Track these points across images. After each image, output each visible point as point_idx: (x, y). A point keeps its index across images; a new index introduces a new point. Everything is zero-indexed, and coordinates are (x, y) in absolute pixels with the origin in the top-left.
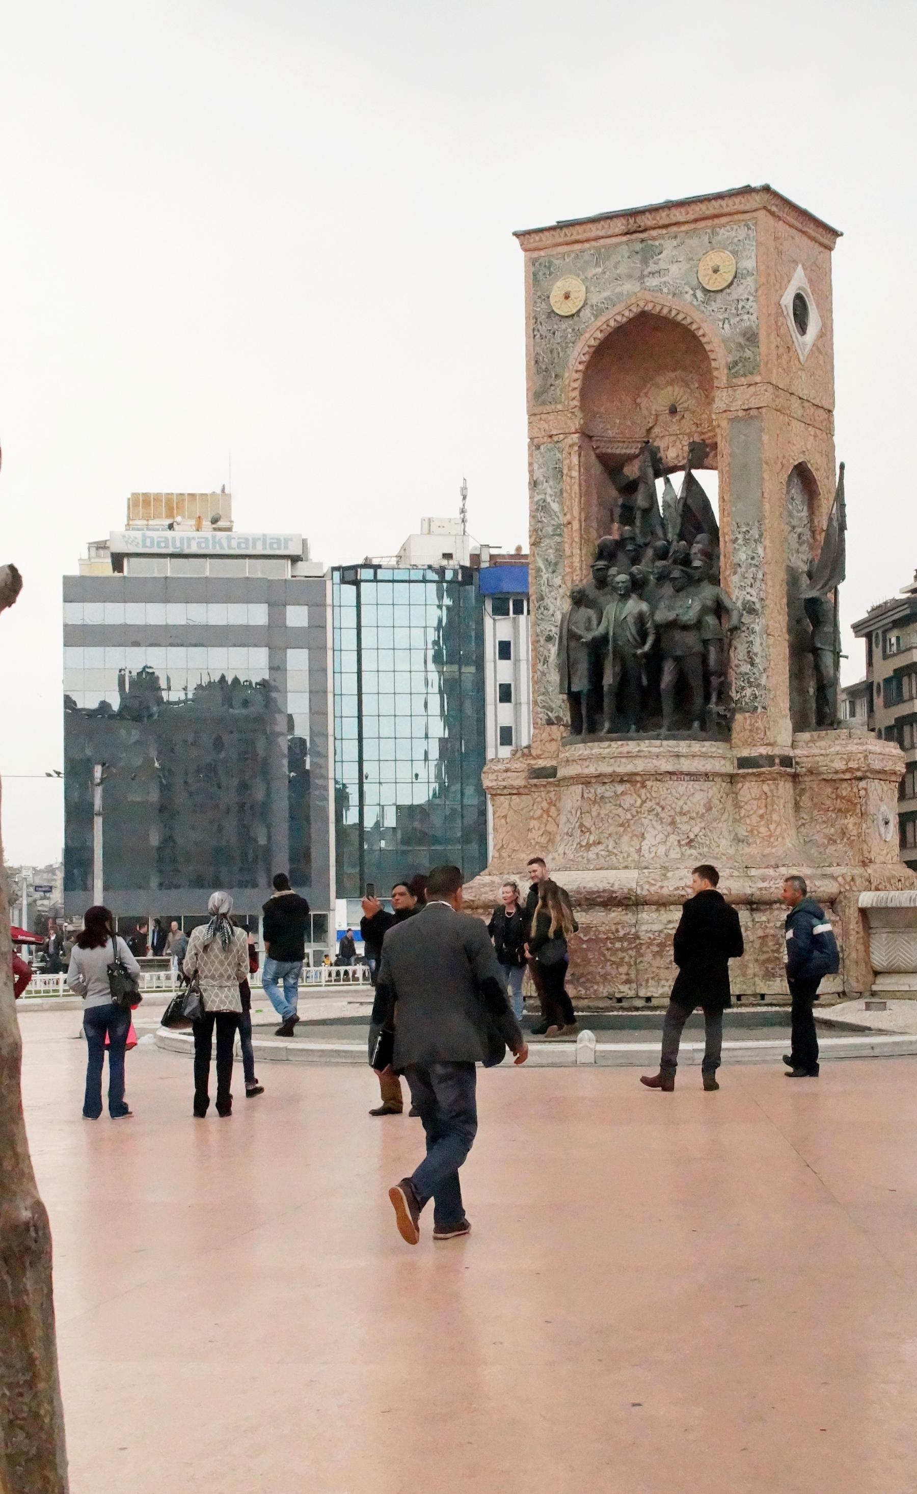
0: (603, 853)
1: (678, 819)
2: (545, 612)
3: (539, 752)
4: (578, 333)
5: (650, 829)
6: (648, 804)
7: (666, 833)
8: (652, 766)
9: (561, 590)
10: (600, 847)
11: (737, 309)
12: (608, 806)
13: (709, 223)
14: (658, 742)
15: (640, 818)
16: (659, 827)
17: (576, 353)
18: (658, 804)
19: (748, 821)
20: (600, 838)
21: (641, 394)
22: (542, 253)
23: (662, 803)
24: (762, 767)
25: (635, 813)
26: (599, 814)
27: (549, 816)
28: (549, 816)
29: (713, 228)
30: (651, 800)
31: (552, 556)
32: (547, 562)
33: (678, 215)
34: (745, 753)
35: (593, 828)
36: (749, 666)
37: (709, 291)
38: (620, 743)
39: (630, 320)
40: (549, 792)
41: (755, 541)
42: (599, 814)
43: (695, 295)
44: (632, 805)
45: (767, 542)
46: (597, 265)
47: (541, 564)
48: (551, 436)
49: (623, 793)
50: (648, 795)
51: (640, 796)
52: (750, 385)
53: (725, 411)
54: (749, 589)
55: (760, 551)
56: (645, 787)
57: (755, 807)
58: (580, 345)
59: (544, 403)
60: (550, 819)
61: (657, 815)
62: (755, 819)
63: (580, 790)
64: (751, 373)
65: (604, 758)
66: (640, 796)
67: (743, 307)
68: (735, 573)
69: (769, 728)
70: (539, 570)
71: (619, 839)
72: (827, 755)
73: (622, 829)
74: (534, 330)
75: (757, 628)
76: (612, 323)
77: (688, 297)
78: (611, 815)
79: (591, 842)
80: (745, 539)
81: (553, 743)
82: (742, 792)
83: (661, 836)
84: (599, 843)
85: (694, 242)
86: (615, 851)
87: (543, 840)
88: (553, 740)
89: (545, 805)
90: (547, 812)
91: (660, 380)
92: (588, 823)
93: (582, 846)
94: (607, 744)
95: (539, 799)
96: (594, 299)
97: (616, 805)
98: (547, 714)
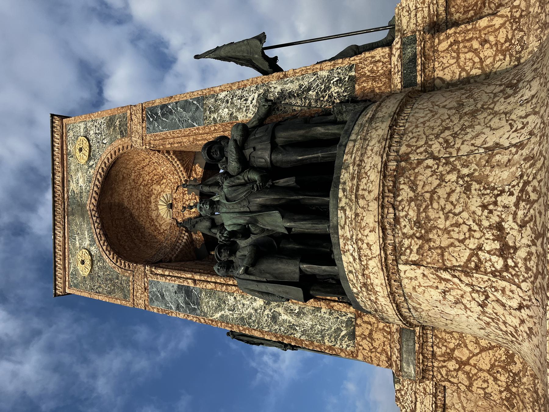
0: (520, 213)
1: (466, 109)
2: (253, 318)
3: (383, 357)
4: (101, 258)
5: (478, 142)
6: (436, 147)
7: (489, 118)
8: (377, 145)
9: (238, 298)
10: (509, 224)
11: (98, 134)
12: (432, 214)
13: (65, 156)
14: (350, 144)
15: (459, 158)
16: (478, 128)
17: (108, 260)
18: (437, 136)
19: (488, 61)
20: (490, 227)
21: (159, 228)
22: (67, 278)
23: (435, 131)
24: (415, 55)
25: (448, 168)
26: (446, 231)
27: (467, 363)
28: (467, 363)
29: (68, 154)
30: (430, 146)
31: (214, 302)
32: (218, 308)
33: (58, 178)
34: (397, 79)
35: (472, 244)
36: (310, 92)
37: (89, 155)
38: (341, 194)
39: (100, 217)
40: (434, 354)
41: (216, 101)
42: (446, 231)
43: (91, 166)
44: (434, 172)
45: (217, 89)
46: (75, 239)
47: (218, 315)
48: (145, 289)
49: (413, 187)
50: (422, 149)
51: (420, 162)
52: (132, 120)
53: (143, 139)
54: (249, 102)
55: (222, 95)
56: (407, 154)
57: (470, 55)
58: (105, 257)
59: (129, 291)
60: (472, 362)
61: (455, 136)
62: (488, 52)
63: (407, 267)
64: (126, 119)
65: (357, 215)
66: (420, 162)
67: (98, 130)
68: (236, 118)
69: (373, 57)
70: (222, 316)
71: (494, 189)
72: (416, 8)
73: (475, 186)
74: (96, 292)
75: (279, 88)
76: (98, 231)
77: (92, 171)
78: (449, 207)
79: (497, 245)
80: (214, 112)
81: (375, 336)
82: (448, 78)
83: (495, 122)
84: (499, 227)
85: (73, 167)
86: (516, 191)
87: (503, 378)
88: (370, 334)
89: (452, 365)
90: (462, 363)
91: (154, 214)
92: (460, 256)
93: (506, 267)
94: (340, 214)
95: (444, 372)
96: (87, 243)
97: (431, 199)
98: (343, 336)
